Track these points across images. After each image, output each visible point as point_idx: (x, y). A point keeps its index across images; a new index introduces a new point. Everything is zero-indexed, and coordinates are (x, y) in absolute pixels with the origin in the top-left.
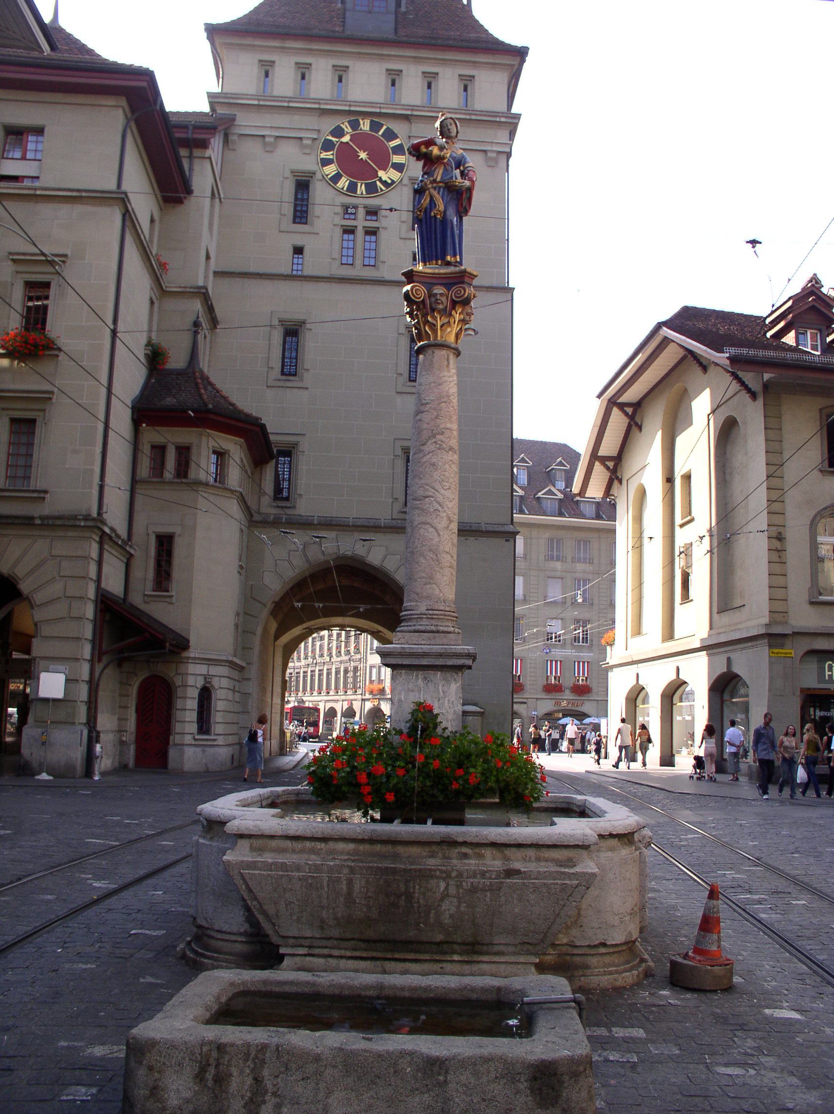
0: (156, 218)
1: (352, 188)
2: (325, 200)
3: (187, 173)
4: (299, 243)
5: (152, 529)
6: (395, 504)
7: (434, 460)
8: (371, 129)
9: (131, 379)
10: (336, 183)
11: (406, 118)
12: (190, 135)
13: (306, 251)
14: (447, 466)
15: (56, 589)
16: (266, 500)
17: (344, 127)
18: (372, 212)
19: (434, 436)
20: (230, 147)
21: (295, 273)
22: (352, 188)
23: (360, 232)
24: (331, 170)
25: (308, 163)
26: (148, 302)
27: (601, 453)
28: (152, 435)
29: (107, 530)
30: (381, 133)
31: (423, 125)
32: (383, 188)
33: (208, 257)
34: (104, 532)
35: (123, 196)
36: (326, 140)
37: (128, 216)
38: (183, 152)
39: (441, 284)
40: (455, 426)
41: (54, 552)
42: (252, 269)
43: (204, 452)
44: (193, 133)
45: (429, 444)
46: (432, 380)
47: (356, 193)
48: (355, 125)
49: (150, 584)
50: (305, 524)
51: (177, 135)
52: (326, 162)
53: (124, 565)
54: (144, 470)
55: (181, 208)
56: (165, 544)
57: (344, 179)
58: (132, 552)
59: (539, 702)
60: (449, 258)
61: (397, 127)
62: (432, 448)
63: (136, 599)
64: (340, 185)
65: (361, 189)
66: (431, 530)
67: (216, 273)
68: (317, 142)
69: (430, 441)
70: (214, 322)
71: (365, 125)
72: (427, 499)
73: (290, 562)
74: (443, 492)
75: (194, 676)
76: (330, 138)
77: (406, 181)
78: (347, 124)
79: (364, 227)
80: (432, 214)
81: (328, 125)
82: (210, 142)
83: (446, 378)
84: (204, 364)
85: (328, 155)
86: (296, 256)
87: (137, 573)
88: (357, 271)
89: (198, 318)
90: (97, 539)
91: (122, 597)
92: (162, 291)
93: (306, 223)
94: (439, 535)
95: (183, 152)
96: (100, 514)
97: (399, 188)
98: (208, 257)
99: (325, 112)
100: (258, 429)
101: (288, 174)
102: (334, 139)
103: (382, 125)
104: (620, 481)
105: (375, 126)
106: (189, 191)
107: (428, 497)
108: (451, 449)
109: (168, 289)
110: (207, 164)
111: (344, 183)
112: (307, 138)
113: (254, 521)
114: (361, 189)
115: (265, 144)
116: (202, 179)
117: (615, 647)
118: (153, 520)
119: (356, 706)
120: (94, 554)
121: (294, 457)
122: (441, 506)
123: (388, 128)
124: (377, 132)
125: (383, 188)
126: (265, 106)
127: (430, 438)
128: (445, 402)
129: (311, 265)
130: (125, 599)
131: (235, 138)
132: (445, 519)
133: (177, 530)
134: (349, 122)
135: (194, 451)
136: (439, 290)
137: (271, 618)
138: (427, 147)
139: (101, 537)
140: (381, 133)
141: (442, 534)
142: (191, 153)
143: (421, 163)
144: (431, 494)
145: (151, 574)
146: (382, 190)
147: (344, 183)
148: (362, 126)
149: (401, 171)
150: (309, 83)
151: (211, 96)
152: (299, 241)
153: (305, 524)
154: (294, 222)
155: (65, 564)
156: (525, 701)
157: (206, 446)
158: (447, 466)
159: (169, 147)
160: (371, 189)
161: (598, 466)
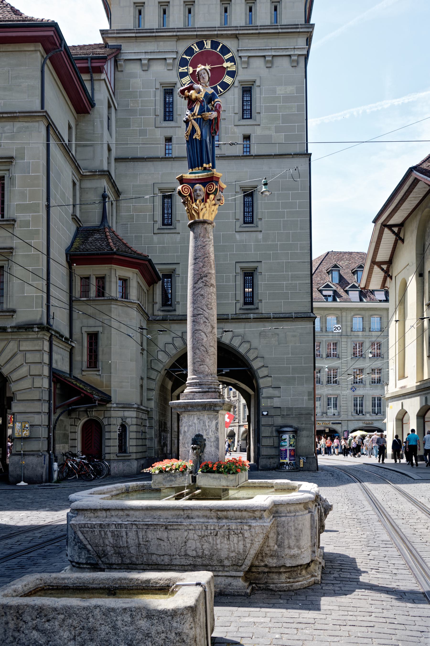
0: (73, 125)
3: (90, 92)
4: (168, 135)
5: (84, 329)
7: (202, 293)
8: (212, 47)
9: (64, 234)
11: (236, 37)
12: (89, 65)
13: (174, 140)
14: (210, 296)
15: (24, 371)
16: (158, 306)
17: (193, 47)
19: (202, 278)
20: (119, 69)
21: (167, 156)
25: (171, 77)
26: (71, 184)
28: (81, 270)
29: (53, 333)
30: (218, 50)
31: (247, 41)
32: (222, 91)
33: (109, 150)
34: (52, 334)
35: (45, 114)
36: (182, 59)
37: (50, 126)
38: (85, 77)
39: (199, 183)
40: (213, 272)
41: (21, 348)
42: (139, 155)
43: (113, 279)
44: (91, 63)
45: (199, 283)
46: (199, 244)
48: (201, 45)
49: (85, 364)
51: (78, 65)
52: (183, 75)
53: (68, 353)
54: (77, 293)
55: (88, 117)
56: (93, 338)
58: (73, 345)
59: (349, 422)
60: (205, 165)
62: (201, 285)
63: (77, 373)
66: (202, 333)
67: (117, 160)
69: (200, 281)
70: (118, 193)
71: (208, 45)
72: (199, 316)
73: (174, 345)
74: (208, 311)
76: (185, 56)
78: (195, 45)
80: (194, 137)
81: (183, 47)
82: (103, 68)
83: (207, 242)
84: (113, 222)
86: (167, 144)
87: (77, 358)
89: (105, 192)
90: (48, 339)
91: (68, 372)
92: (81, 174)
93: (172, 120)
94: (207, 336)
95: (85, 77)
96: (48, 322)
97: (232, 89)
98: (109, 150)
99: (179, 38)
100: (147, 263)
101: (158, 86)
103: (219, 43)
105: (215, 45)
106: (93, 105)
107: (198, 315)
108: (212, 285)
109: (84, 174)
110: (103, 83)
112: (170, 58)
113: (150, 320)
115: (142, 65)
116: (101, 95)
117: (389, 386)
118: (83, 325)
119: (236, 430)
120: (47, 348)
122: (207, 319)
123: (223, 46)
124: (216, 49)
125: (222, 91)
126: (141, 35)
127: (199, 279)
128: (207, 257)
130: (70, 374)
132: (210, 327)
133: (100, 329)
134: (197, 43)
135: (107, 279)
136: (198, 186)
137: (167, 379)
138: (189, 92)
139: (50, 337)
140: (218, 50)
141: (208, 335)
142: (92, 77)
143: (187, 101)
144: (201, 313)
145: (85, 358)
146: (221, 92)
148: (206, 45)
149: (233, 77)
150: (169, 16)
151: (103, 32)
154: (165, 120)
155: (28, 355)
156: (340, 422)
157: (116, 273)
158: (210, 296)
159: (76, 73)
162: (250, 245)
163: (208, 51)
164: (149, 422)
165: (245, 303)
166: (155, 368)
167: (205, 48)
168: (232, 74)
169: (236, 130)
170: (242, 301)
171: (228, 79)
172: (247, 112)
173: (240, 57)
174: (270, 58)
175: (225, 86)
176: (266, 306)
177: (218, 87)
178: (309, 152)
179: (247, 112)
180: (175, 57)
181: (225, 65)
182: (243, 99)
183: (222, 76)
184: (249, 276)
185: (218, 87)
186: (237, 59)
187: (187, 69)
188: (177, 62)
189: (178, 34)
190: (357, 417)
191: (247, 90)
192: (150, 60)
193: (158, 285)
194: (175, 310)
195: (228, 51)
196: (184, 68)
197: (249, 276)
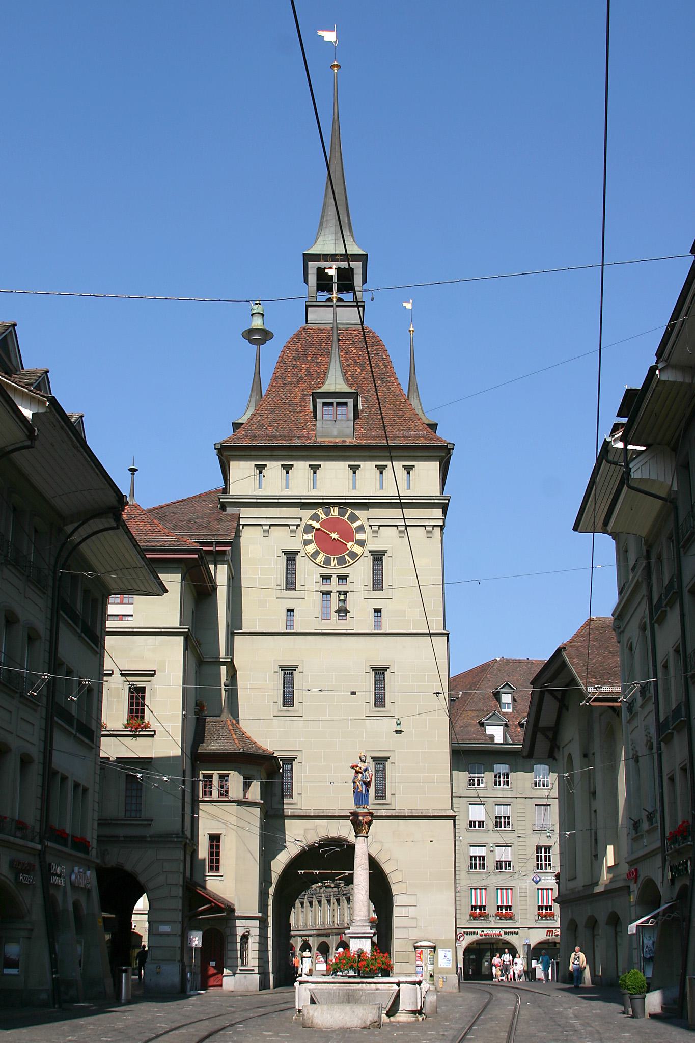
1: (327, 562)
18: (343, 578)
24: (312, 548)
25: (295, 544)
27: (542, 723)
52: (307, 543)
57: (321, 555)
64: (318, 560)
65: (334, 562)
71: (335, 512)
75: (241, 927)
77: (367, 553)
85: (309, 537)
104: (558, 748)
111: (321, 558)
114: (334, 562)
147: (321, 558)
149: (363, 546)
160: (341, 561)
161: (539, 736)
168: (361, 543)
172: (378, 584)
175: (353, 555)
177: (347, 557)
179: (378, 584)
185: (347, 557)
186: (367, 528)
188: (301, 528)
190: (476, 924)
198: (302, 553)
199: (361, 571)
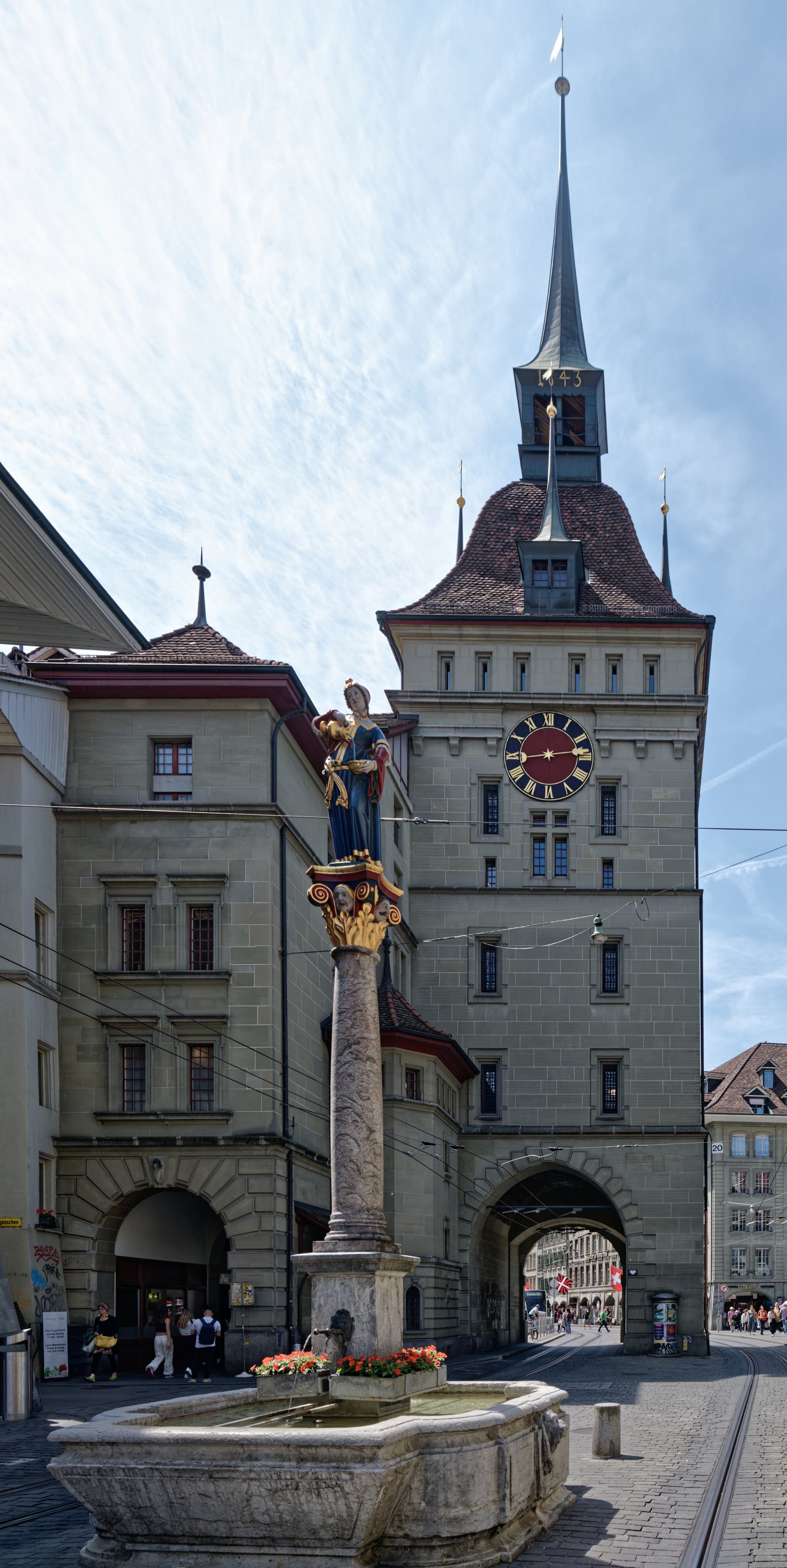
1: (540, 792)
2: (515, 806)
4: (491, 854)
6: (593, 1112)
8: (556, 724)
10: (523, 788)
16: (475, 1112)
17: (528, 723)
20: (416, 752)
22: (540, 792)
23: (550, 840)
24: (517, 772)
25: (494, 766)
30: (565, 728)
31: (608, 717)
36: (511, 739)
42: (446, 884)
47: (543, 797)
48: (539, 720)
50: (511, 1133)
52: (512, 764)
57: (531, 782)
61: (581, 720)
65: (549, 792)
68: (503, 742)
76: (515, 737)
77: (592, 781)
79: (553, 834)
81: (511, 722)
88: (549, 879)
97: (587, 788)
101: (475, 780)
102: (519, 738)
103: (567, 719)
105: (560, 720)
112: (492, 738)
114: (549, 792)
115: (450, 747)
121: (498, 1071)
123: (573, 722)
129: (502, 877)
131: (420, 742)
134: (533, 717)
140: (565, 728)
146: (569, 792)
149: (587, 770)
150: (491, 675)
151: (390, 694)
152: (491, 852)
153: (511, 1133)
160: (559, 792)
162: (610, 1022)
163: (549, 730)
164: (462, 1284)
165: (605, 1110)
166: (471, 1204)
167: (546, 725)
168: (586, 766)
169: (591, 851)
170: (600, 1107)
171: (579, 774)
173: (598, 741)
174: (643, 745)
175: (575, 783)
176: (635, 1114)
177: (566, 785)
178: (700, 888)
180: (500, 736)
181: (576, 751)
182: (603, 804)
183: (571, 769)
184: (611, 1070)
185: (566, 785)
187: (518, 755)
189: (505, 701)
191: (609, 792)
192: (462, 739)
193: (475, 1080)
194: (500, 1119)
195: (580, 731)
196: (514, 754)
197: (611, 1070)
198: (506, 780)
199: (584, 806)
